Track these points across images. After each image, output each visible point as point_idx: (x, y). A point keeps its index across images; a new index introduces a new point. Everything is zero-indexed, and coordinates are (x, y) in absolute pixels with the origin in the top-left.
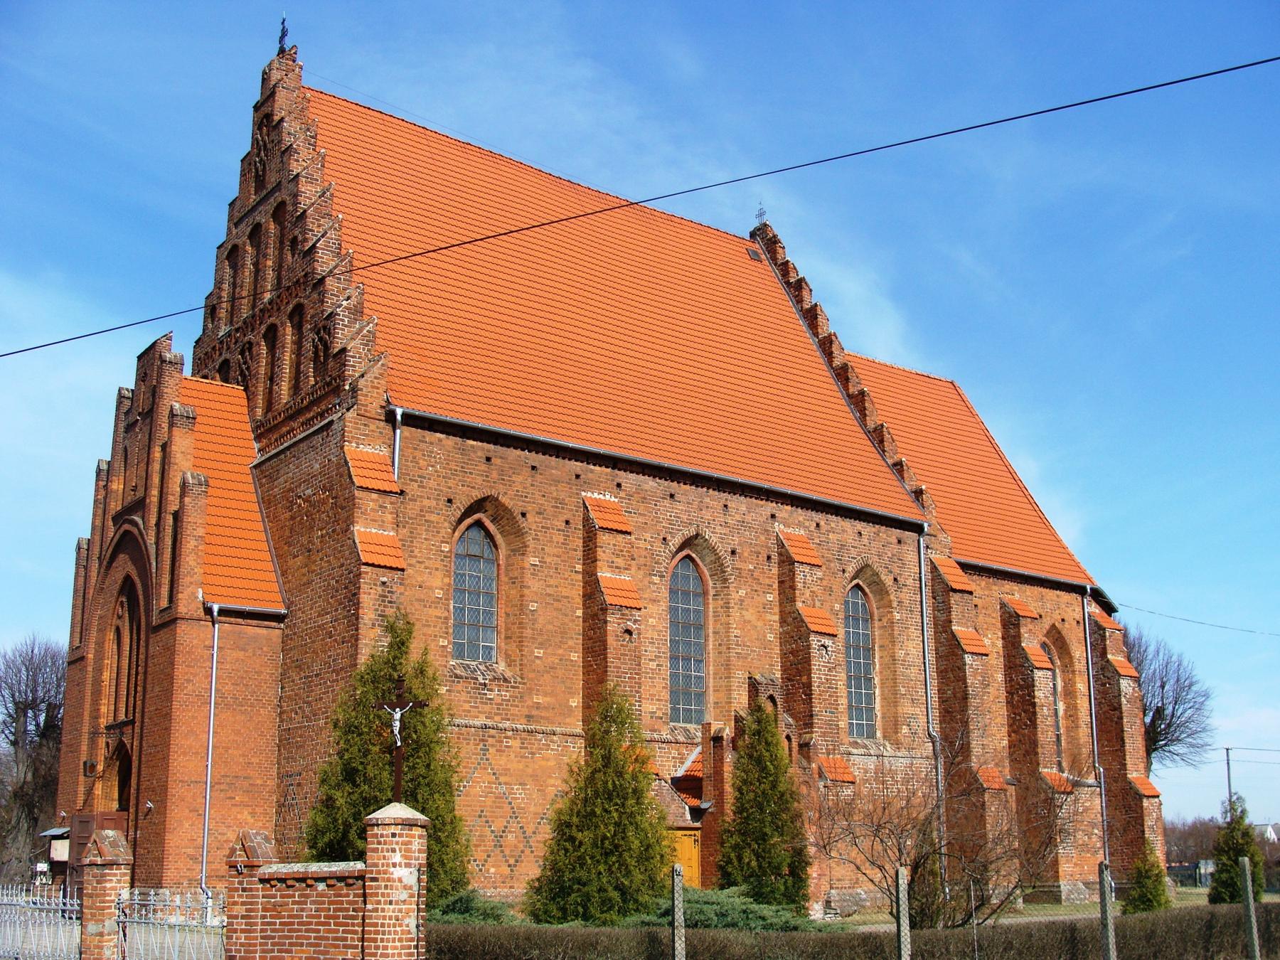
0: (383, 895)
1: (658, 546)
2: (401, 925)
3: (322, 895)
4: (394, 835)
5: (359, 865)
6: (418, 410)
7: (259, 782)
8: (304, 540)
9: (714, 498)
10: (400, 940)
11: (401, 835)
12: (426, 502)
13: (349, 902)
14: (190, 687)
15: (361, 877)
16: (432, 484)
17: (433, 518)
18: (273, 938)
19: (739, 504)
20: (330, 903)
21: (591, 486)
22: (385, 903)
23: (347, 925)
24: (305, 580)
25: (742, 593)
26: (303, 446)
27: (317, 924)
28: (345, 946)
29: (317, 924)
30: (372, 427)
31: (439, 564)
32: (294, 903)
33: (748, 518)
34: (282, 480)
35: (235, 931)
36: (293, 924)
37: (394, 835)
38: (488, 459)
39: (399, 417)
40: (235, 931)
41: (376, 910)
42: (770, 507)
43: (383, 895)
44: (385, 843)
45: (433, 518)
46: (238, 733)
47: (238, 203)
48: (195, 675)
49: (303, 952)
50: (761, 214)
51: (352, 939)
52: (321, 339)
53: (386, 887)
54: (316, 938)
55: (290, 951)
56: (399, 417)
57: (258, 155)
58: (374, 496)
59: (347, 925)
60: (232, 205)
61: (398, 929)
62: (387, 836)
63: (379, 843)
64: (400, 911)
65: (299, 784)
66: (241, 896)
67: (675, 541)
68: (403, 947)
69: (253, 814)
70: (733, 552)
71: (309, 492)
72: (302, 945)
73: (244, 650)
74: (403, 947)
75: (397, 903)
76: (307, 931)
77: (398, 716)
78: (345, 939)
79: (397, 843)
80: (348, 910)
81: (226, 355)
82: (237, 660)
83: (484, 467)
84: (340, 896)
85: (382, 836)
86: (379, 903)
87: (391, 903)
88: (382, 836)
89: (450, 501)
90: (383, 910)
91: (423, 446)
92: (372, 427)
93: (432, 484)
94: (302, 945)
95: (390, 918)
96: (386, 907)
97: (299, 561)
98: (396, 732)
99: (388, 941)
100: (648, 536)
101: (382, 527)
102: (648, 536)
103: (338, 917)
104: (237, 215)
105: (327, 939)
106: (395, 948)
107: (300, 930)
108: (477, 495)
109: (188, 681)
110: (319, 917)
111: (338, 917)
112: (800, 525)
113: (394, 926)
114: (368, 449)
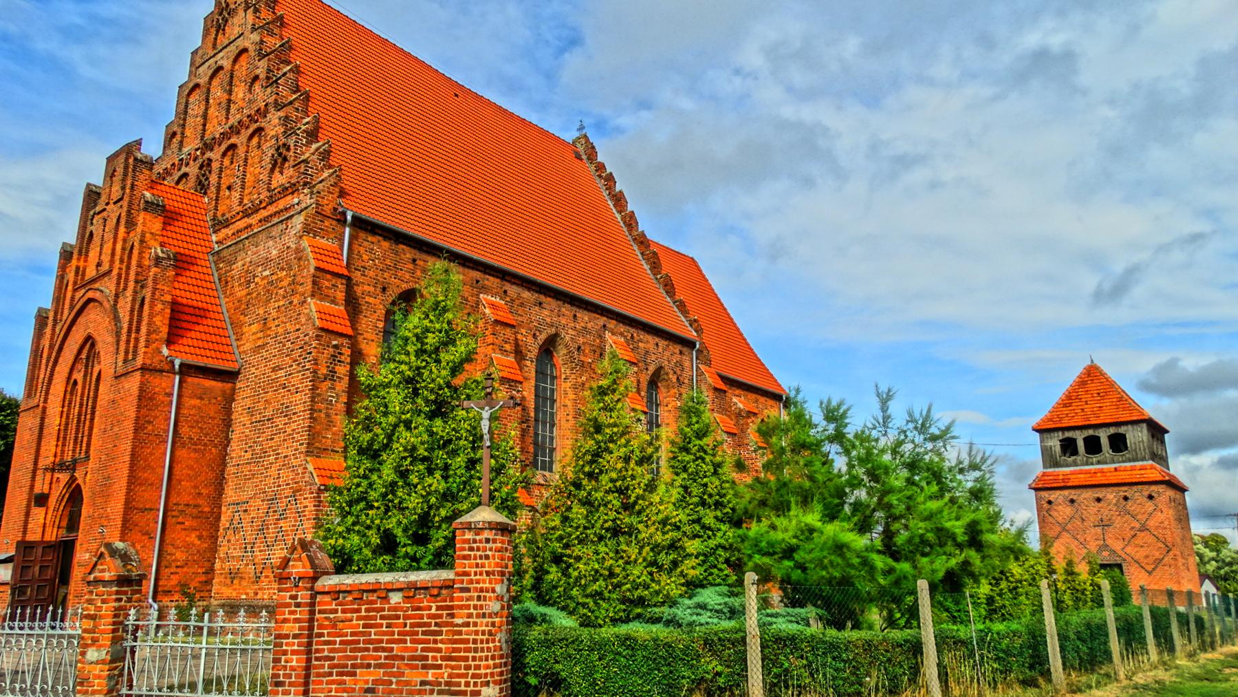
0: (475, 607)
1: (530, 340)
2: (494, 641)
3: (395, 609)
4: (488, 541)
5: (445, 575)
6: (365, 215)
7: (207, 509)
8: (261, 311)
9: (567, 310)
10: (493, 658)
11: (494, 541)
12: (366, 287)
13: (429, 616)
14: (150, 427)
15: (449, 586)
16: (372, 273)
17: (371, 300)
18: (333, 658)
19: (584, 316)
20: (406, 617)
21: (485, 289)
22: (478, 616)
23: (428, 642)
24: (260, 343)
25: (584, 378)
26: (262, 236)
27: (389, 642)
28: (424, 667)
29: (389, 642)
30: (327, 223)
31: (374, 337)
32: (359, 618)
33: (589, 325)
34: (240, 264)
35: (285, 653)
36: (358, 642)
37: (488, 541)
38: (414, 260)
39: (349, 218)
40: (285, 653)
41: (467, 624)
42: (602, 320)
43: (475, 607)
44: (478, 549)
45: (371, 300)
46: (191, 468)
47: (200, 52)
48: (156, 417)
49: (370, 674)
50: (581, 128)
51: (435, 658)
52: (280, 154)
53: (479, 598)
54: (386, 658)
55: (354, 674)
56: (349, 218)
57: (221, 14)
58: (329, 277)
59: (428, 642)
60: (194, 53)
61: (491, 645)
62: (481, 541)
63: (471, 549)
64: (493, 624)
65: (246, 511)
66: (291, 613)
67: (542, 337)
68: (495, 666)
69: (200, 537)
70: (579, 348)
71: (267, 273)
72: (369, 666)
73: (201, 399)
74: (495, 666)
75: (490, 616)
76: (376, 650)
77: (486, 414)
78: (426, 658)
79: (491, 549)
80: (429, 625)
81: (184, 169)
82: (194, 406)
83: (411, 266)
84: (419, 609)
85: (475, 541)
86: (470, 616)
87: (484, 615)
88: (475, 541)
89: (384, 289)
90: (475, 624)
91: (366, 244)
92: (327, 223)
93: (372, 273)
94: (369, 666)
95: (483, 633)
96: (478, 620)
97: (254, 328)
98: (485, 431)
99: (481, 659)
100: (523, 331)
101: (333, 302)
102: (523, 331)
103: (417, 633)
104: (199, 61)
105: (403, 658)
106: (487, 667)
107: (367, 650)
108: (405, 286)
109: (149, 422)
110: (393, 633)
111: (417, 633)
112: (622, 334)
113: (487, 642)
114: (324, 241)
